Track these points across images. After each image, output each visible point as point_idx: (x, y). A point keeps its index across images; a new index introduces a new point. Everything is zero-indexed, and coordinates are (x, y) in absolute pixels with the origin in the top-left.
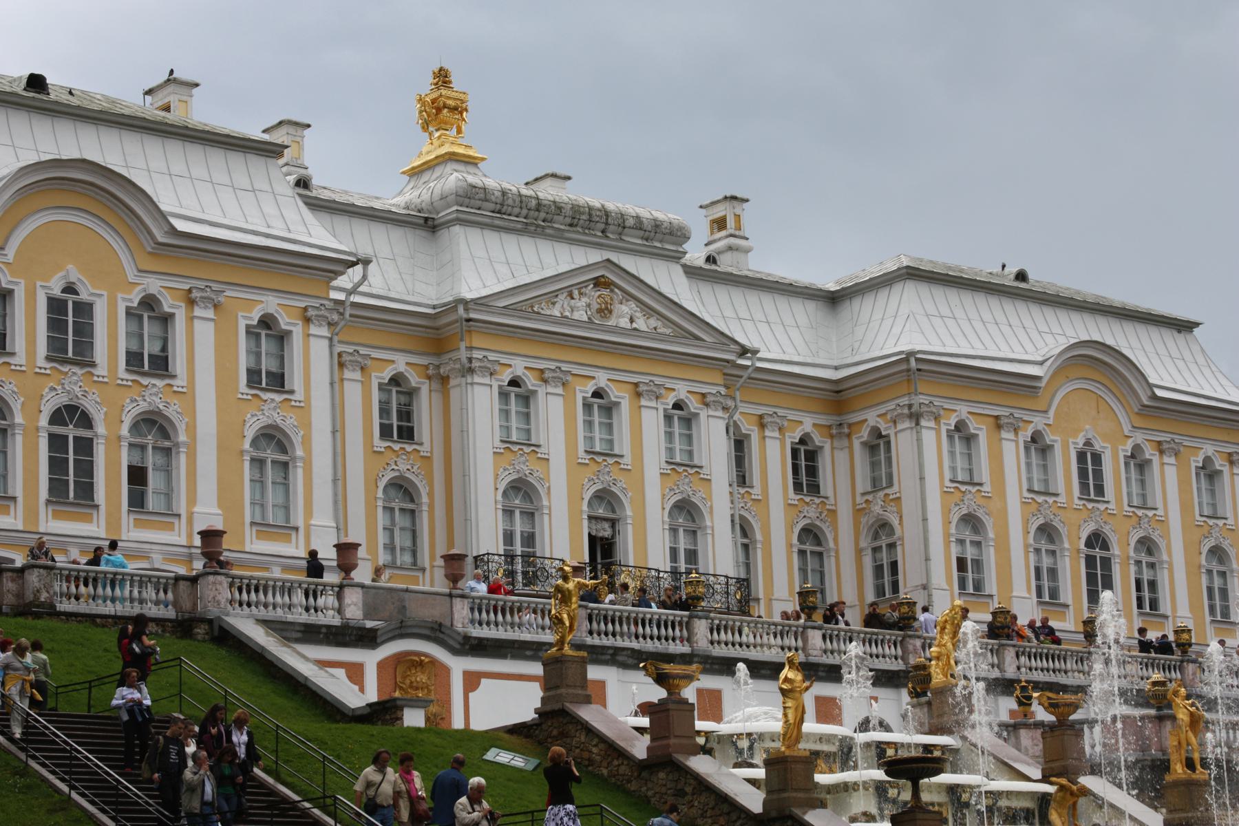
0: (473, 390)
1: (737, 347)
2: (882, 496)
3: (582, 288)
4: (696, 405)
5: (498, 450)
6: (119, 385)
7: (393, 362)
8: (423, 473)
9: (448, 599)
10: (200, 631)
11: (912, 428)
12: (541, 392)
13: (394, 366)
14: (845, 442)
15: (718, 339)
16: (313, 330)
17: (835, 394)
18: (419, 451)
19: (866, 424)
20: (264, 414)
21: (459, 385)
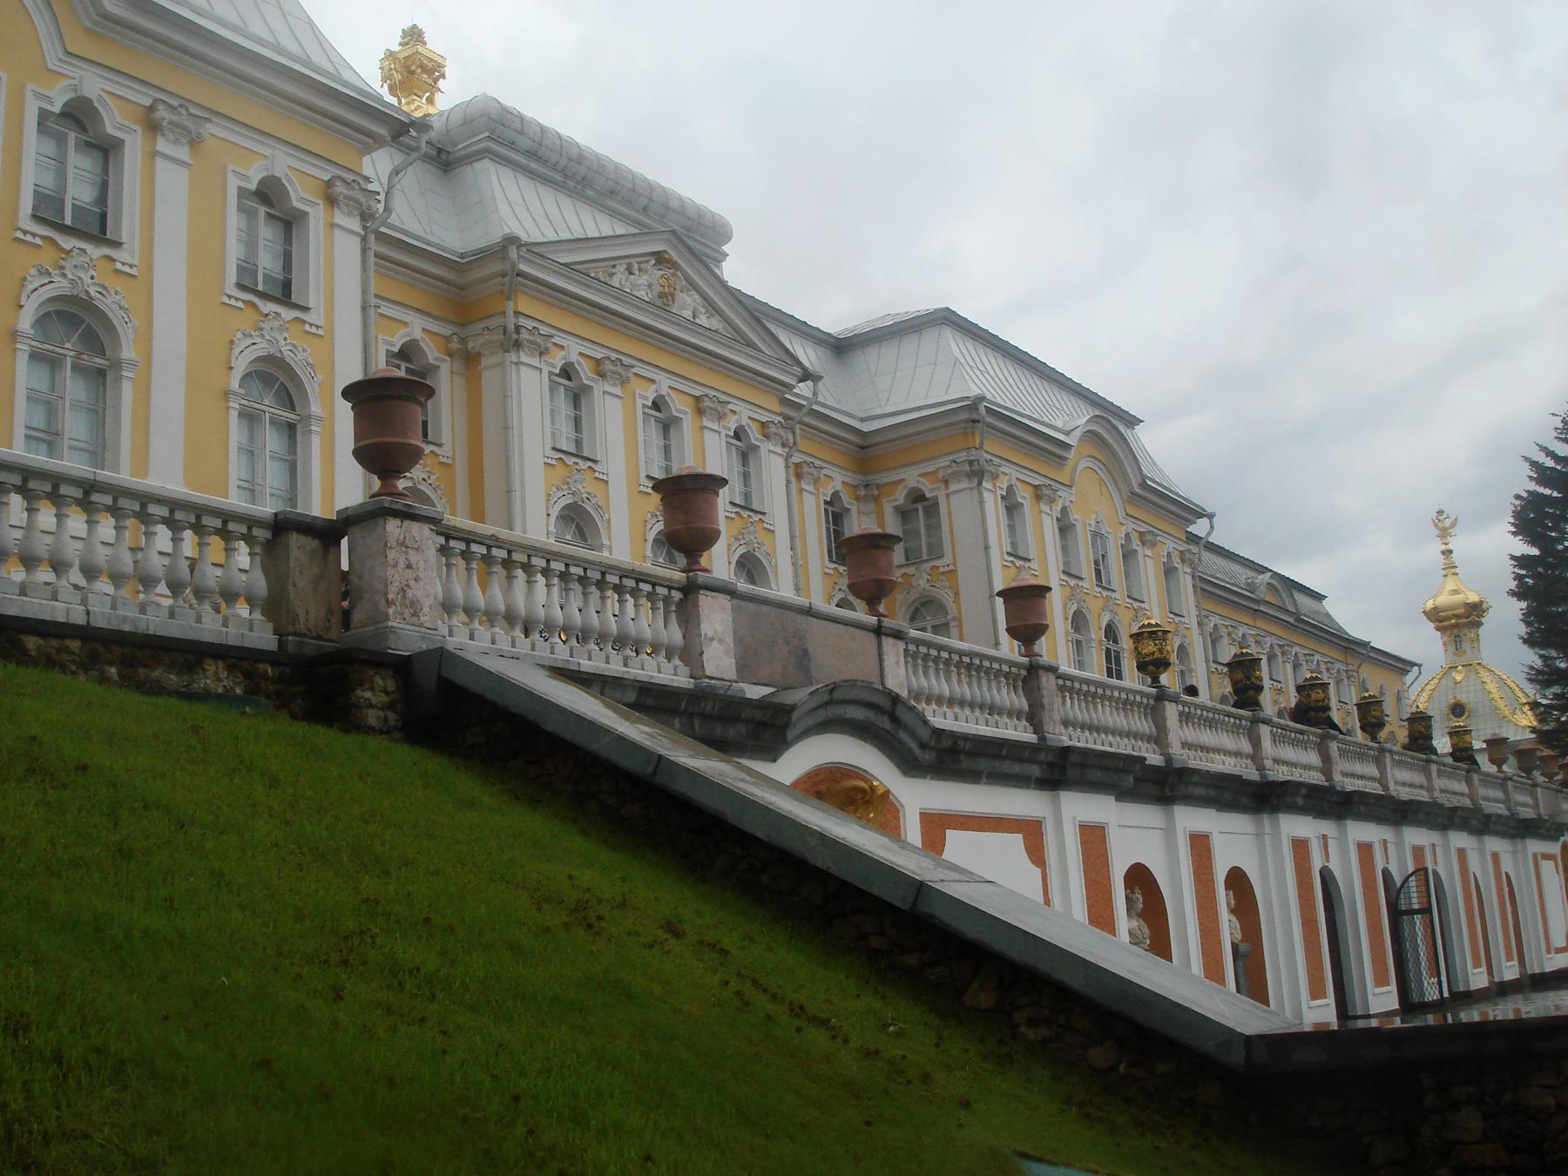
0: (519, 376)
1: (799, 370)
2: (928, 569)
3: (641, 262)
4: (757, 436)
5: (549, 461)
6: (17, 239)
7: (406, 324)
8: (442, 486)
9: (872, 636)
10: (374, 694)
11: (971, 489)
12: (599, 387)
13: (408, 330)
14: (872, 506)
15: (777, 354)
16: (340, 218)
17: (859, 449)
18: (438, 455)
19: (903, 484)
20: (263, 336)
21: (501, 364)
